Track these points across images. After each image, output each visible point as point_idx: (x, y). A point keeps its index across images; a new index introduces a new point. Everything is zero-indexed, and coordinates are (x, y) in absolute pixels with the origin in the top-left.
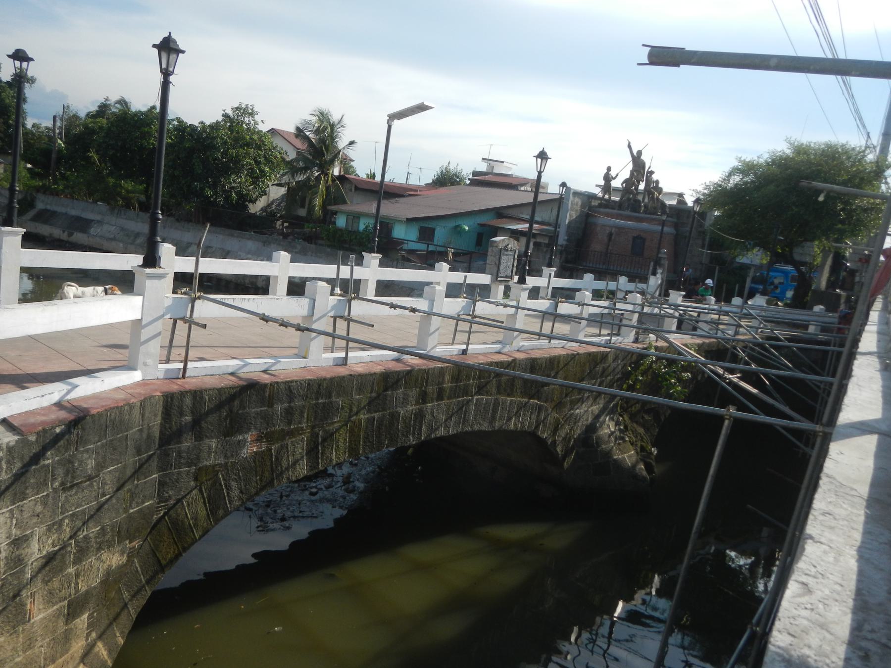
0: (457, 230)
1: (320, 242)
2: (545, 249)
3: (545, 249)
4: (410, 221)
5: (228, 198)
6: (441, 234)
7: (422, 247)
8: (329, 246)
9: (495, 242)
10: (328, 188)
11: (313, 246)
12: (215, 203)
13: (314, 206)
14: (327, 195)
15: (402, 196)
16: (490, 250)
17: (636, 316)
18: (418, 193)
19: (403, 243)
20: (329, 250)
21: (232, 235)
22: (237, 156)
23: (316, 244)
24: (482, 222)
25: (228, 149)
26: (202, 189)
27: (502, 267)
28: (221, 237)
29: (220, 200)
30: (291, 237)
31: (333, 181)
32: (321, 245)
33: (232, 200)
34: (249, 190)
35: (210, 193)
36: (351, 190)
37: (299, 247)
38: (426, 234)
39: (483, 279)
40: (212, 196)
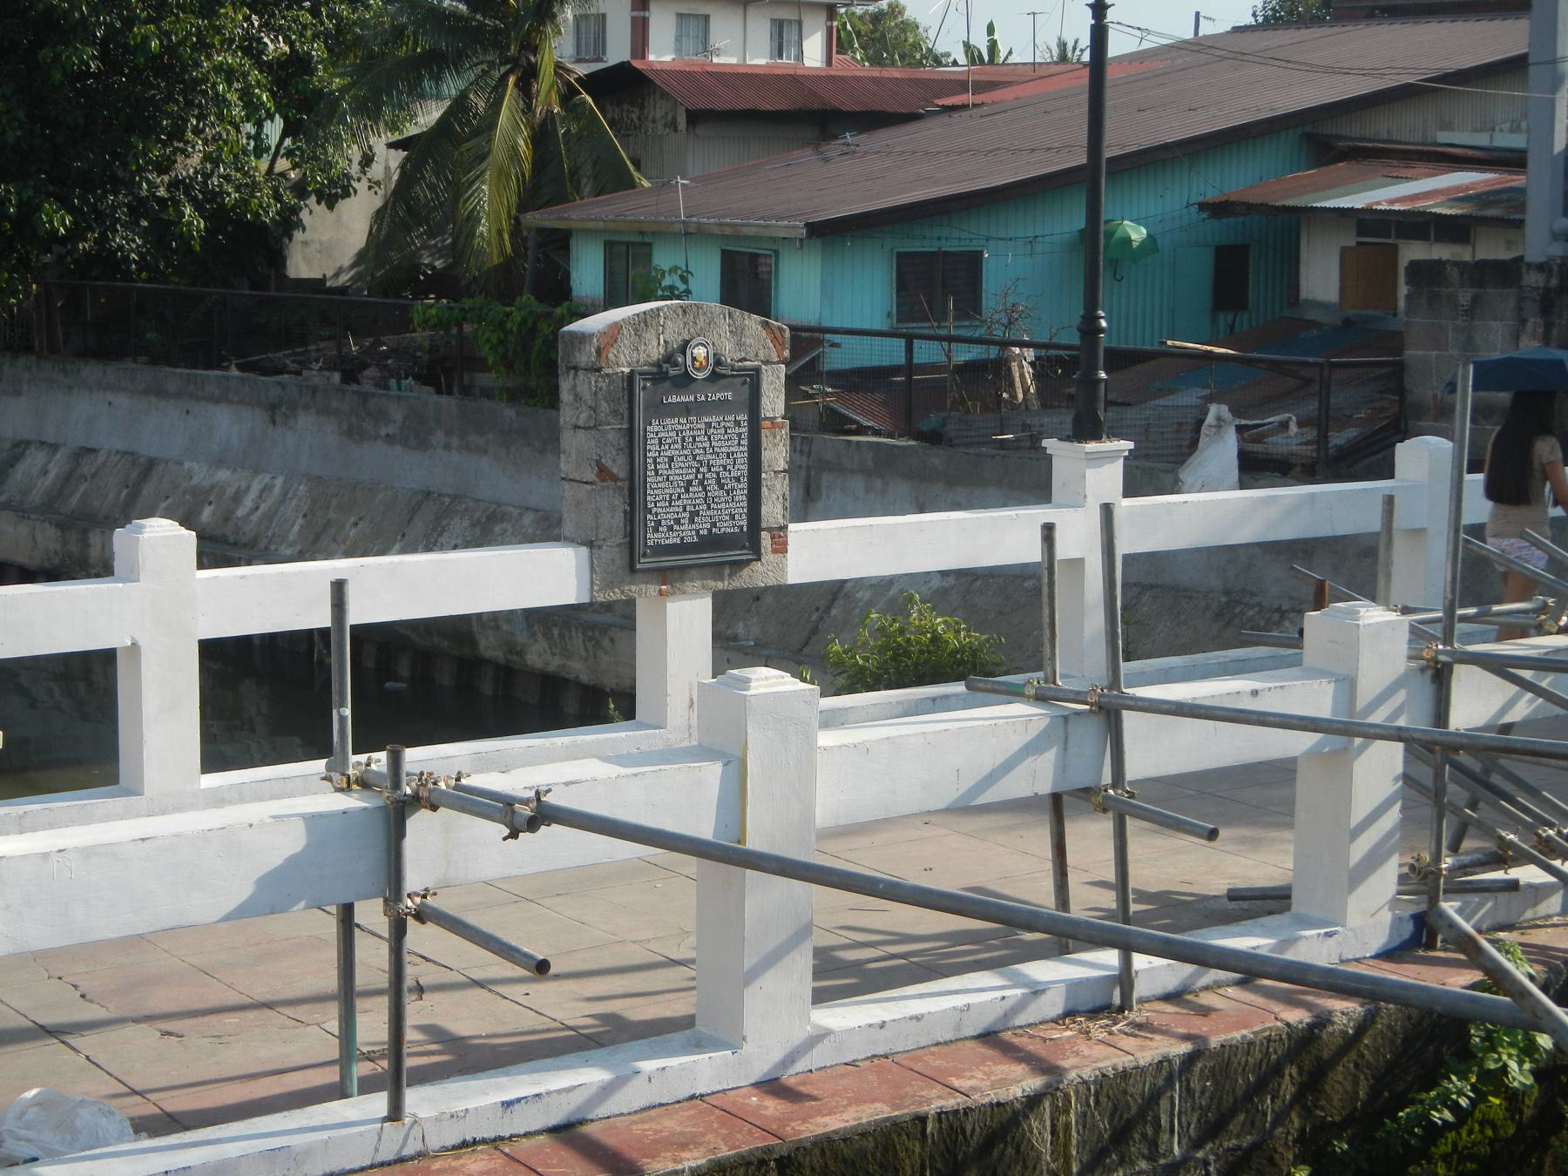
0: (1094, 252)
1: (484, 379)
2: (1465, 297)
3: (1465, 297)
4: (829, 233)
5: (163, 230)
6: (1019, 270)
7: (890, 353)
8: (513, 396)
9: (583, 338)
10: (542, 136)
11: (448, 404)
12: (107, 262)
13: (473, 219)
14: (539, 164)
15: (912, 117)
16: (565, 385)
17: (1379, 769)
18: (969, 98)
19: (820, 342)
20: (509, 413)
21: (160, 392)
22: (169, 49)
23: (466, 391)
24: (1212, 195)
25: (129, 22)
26: (29, 209)
27: (657, 490)
28: (122, 401)
29: (129, 242)
30: (372, 372)
31: (568, 95)
32: (487, 393)
33: (185, 240)
34: (254, 186)
35: (62, 222)
36: (673, 125)
37: (398, 413)
38: (937, 282)
39: (536, 576)
40: (76, 233)
